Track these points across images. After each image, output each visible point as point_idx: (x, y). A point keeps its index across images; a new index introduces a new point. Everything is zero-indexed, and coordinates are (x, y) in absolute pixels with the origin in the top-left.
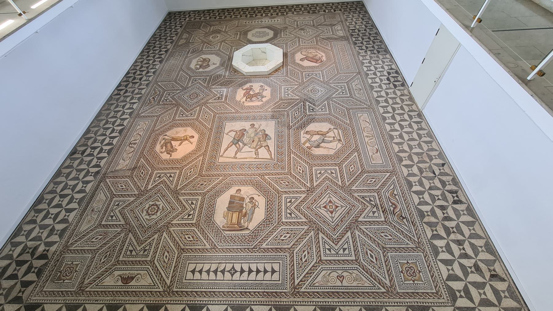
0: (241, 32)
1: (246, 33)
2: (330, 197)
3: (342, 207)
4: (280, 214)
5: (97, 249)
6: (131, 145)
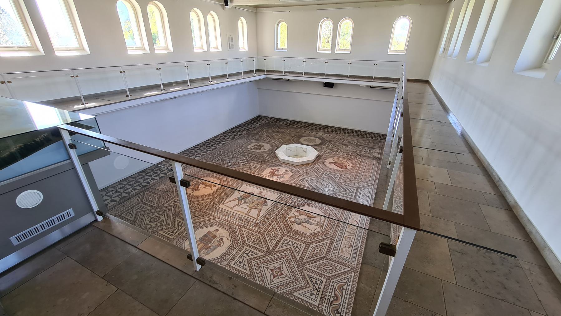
1: (300, 138)
2: (282, 264)
3: (286, 276)
4: (232, 259)
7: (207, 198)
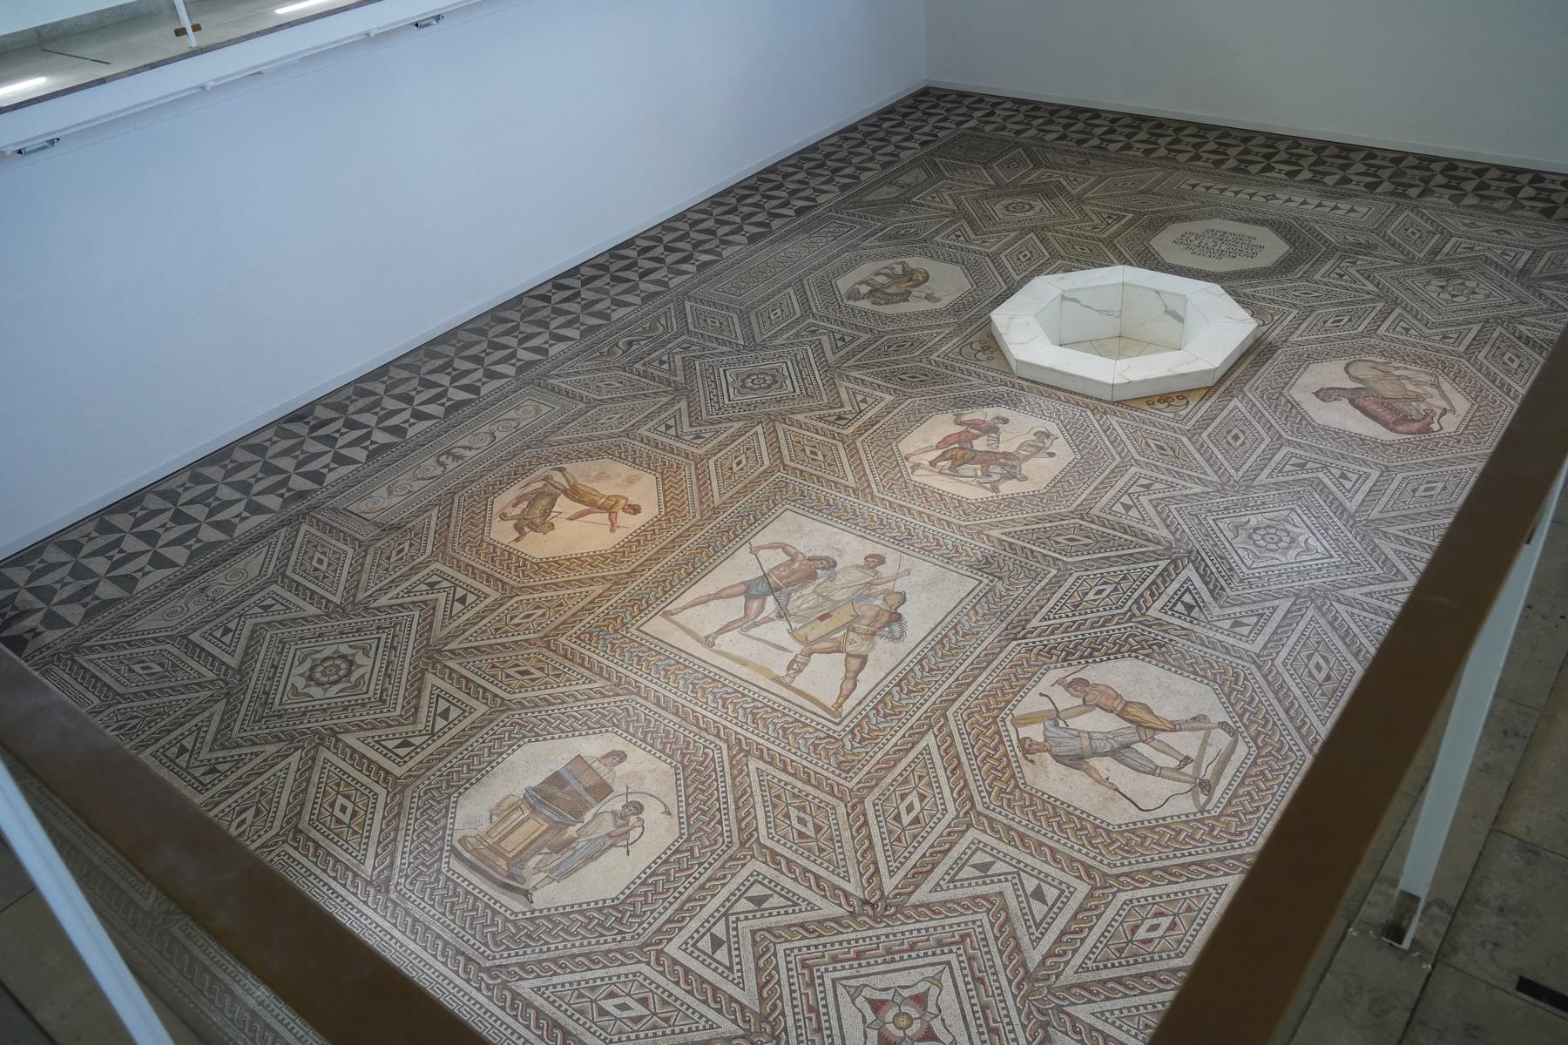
0: (1138, 215)
4: (677, 921)
5: (122, 696)
6: (443, 459)
7: (585, 574)
